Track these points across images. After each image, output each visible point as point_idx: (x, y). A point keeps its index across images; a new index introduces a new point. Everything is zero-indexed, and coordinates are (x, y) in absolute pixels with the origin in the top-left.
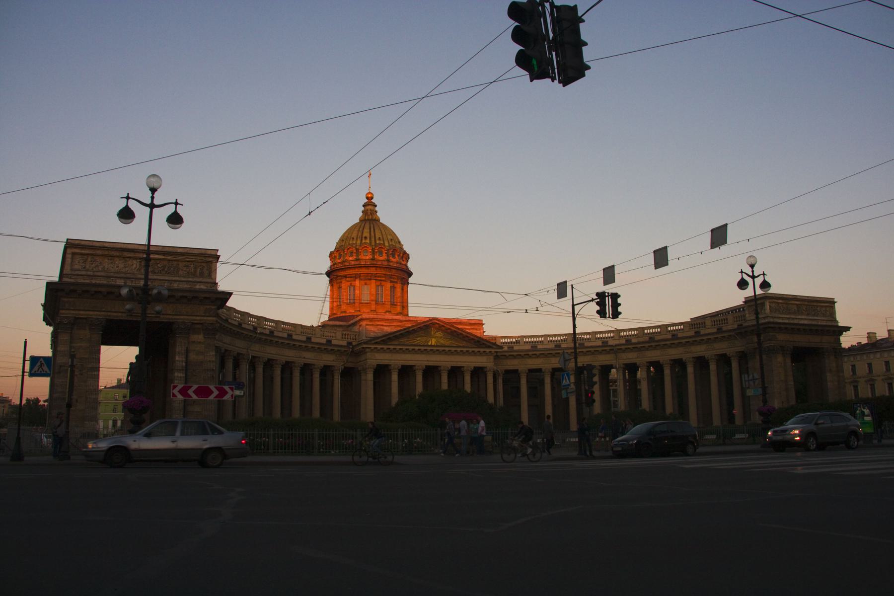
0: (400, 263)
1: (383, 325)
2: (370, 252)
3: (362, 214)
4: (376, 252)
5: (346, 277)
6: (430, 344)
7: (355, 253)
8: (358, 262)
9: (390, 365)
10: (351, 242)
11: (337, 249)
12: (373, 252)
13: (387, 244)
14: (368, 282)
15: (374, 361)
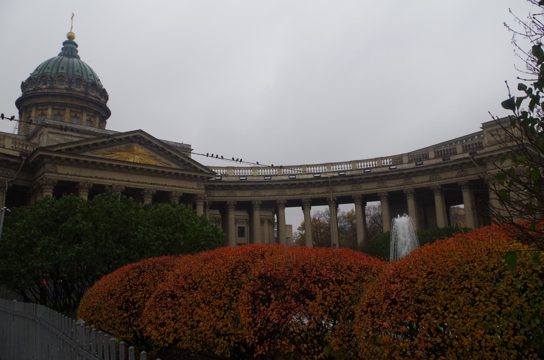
0: (99, 99)
1: (72, 136)
2: (67, 82)
3: (61, 51)
4: (73, 83)
5: (37, 105)
6: (132, 161)
7: (49, 81)
8: (52, 91)
9: (78, 183)
10: (46, 71)
11: (30, 79)
12: (70, 82)
13: (85, 77)
14: (62, 113)
15: (56, 175)
